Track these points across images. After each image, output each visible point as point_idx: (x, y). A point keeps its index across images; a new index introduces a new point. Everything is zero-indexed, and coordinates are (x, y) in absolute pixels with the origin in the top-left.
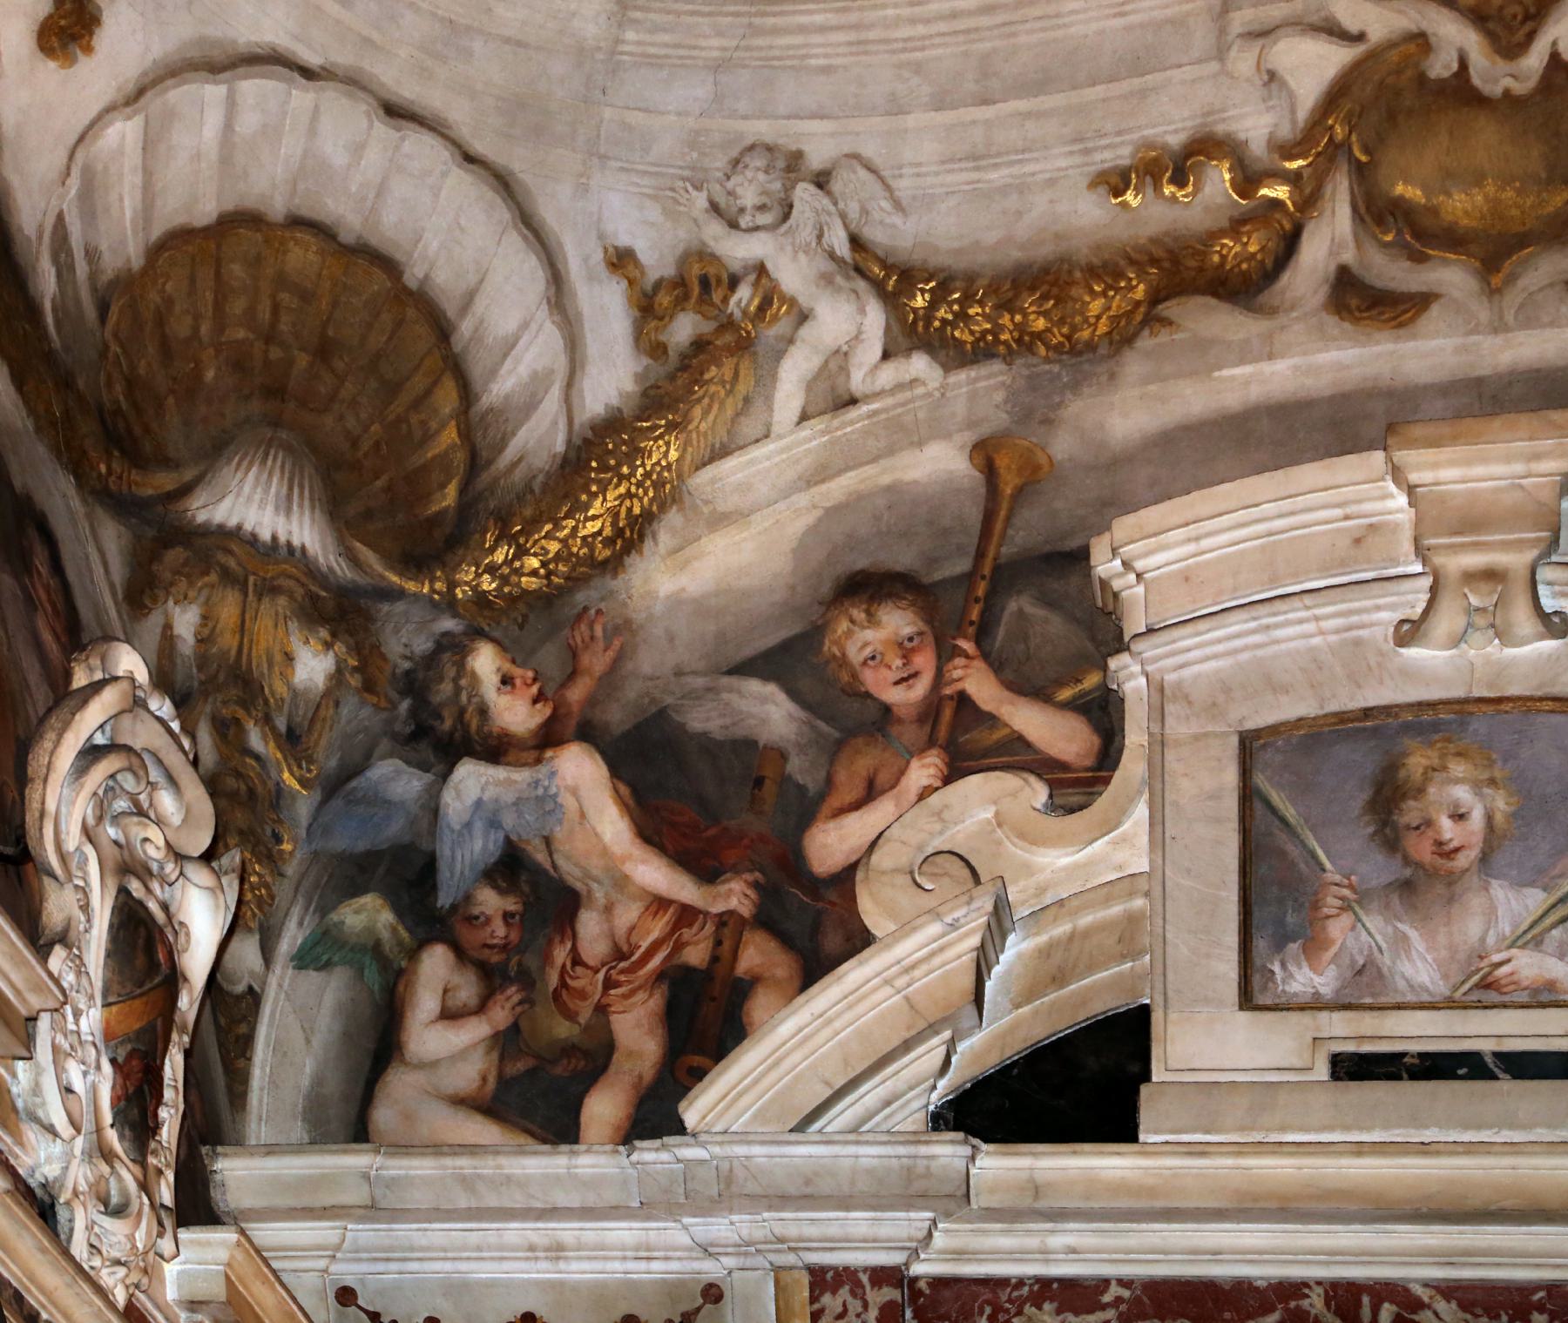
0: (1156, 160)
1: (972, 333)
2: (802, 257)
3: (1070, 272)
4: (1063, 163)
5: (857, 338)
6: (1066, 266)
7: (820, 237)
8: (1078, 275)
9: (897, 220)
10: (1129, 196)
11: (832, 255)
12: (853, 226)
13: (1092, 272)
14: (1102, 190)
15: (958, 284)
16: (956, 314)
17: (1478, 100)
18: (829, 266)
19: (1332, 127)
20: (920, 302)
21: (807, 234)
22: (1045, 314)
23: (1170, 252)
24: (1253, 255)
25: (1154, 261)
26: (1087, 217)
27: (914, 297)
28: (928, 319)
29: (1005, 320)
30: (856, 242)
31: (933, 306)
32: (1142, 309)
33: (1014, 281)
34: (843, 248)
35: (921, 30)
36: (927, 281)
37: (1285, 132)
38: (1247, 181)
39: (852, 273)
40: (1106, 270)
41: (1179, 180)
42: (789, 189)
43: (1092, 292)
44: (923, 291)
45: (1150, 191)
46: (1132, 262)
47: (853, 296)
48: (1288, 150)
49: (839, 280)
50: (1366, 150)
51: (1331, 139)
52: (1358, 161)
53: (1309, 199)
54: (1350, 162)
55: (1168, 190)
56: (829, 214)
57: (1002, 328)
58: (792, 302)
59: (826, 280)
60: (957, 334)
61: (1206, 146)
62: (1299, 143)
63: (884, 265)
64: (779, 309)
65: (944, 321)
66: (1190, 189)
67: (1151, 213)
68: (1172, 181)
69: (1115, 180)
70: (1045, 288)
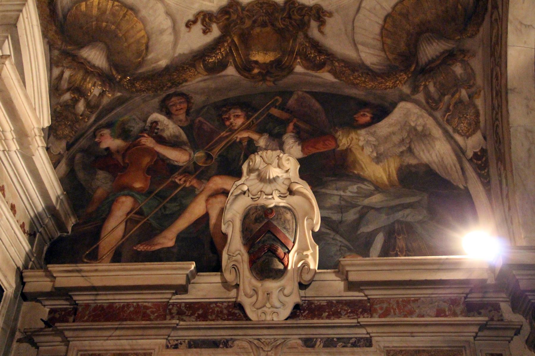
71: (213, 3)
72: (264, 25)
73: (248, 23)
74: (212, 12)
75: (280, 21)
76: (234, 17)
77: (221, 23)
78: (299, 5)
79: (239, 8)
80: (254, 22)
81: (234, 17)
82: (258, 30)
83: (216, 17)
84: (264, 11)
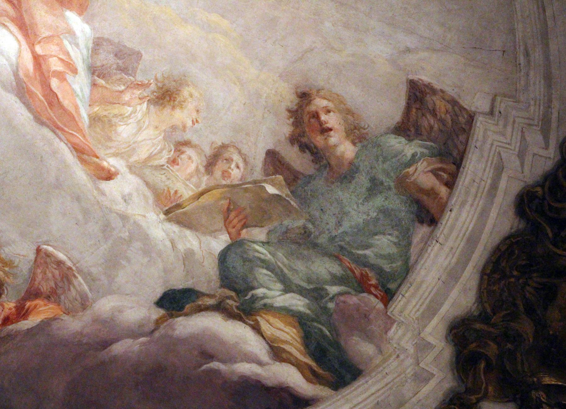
71: (433, 375)
72: (549, 294)
73: (526, 327)
74: (451, 390)
75: (559, 252)
76: (492, 349)
77: (490, 389)
78: (542, 186)
79: (478, 326)
80: (530, 310)
81: (492, 349)
82: (554, 315)
83: (468, 391)
84: (515, 273)
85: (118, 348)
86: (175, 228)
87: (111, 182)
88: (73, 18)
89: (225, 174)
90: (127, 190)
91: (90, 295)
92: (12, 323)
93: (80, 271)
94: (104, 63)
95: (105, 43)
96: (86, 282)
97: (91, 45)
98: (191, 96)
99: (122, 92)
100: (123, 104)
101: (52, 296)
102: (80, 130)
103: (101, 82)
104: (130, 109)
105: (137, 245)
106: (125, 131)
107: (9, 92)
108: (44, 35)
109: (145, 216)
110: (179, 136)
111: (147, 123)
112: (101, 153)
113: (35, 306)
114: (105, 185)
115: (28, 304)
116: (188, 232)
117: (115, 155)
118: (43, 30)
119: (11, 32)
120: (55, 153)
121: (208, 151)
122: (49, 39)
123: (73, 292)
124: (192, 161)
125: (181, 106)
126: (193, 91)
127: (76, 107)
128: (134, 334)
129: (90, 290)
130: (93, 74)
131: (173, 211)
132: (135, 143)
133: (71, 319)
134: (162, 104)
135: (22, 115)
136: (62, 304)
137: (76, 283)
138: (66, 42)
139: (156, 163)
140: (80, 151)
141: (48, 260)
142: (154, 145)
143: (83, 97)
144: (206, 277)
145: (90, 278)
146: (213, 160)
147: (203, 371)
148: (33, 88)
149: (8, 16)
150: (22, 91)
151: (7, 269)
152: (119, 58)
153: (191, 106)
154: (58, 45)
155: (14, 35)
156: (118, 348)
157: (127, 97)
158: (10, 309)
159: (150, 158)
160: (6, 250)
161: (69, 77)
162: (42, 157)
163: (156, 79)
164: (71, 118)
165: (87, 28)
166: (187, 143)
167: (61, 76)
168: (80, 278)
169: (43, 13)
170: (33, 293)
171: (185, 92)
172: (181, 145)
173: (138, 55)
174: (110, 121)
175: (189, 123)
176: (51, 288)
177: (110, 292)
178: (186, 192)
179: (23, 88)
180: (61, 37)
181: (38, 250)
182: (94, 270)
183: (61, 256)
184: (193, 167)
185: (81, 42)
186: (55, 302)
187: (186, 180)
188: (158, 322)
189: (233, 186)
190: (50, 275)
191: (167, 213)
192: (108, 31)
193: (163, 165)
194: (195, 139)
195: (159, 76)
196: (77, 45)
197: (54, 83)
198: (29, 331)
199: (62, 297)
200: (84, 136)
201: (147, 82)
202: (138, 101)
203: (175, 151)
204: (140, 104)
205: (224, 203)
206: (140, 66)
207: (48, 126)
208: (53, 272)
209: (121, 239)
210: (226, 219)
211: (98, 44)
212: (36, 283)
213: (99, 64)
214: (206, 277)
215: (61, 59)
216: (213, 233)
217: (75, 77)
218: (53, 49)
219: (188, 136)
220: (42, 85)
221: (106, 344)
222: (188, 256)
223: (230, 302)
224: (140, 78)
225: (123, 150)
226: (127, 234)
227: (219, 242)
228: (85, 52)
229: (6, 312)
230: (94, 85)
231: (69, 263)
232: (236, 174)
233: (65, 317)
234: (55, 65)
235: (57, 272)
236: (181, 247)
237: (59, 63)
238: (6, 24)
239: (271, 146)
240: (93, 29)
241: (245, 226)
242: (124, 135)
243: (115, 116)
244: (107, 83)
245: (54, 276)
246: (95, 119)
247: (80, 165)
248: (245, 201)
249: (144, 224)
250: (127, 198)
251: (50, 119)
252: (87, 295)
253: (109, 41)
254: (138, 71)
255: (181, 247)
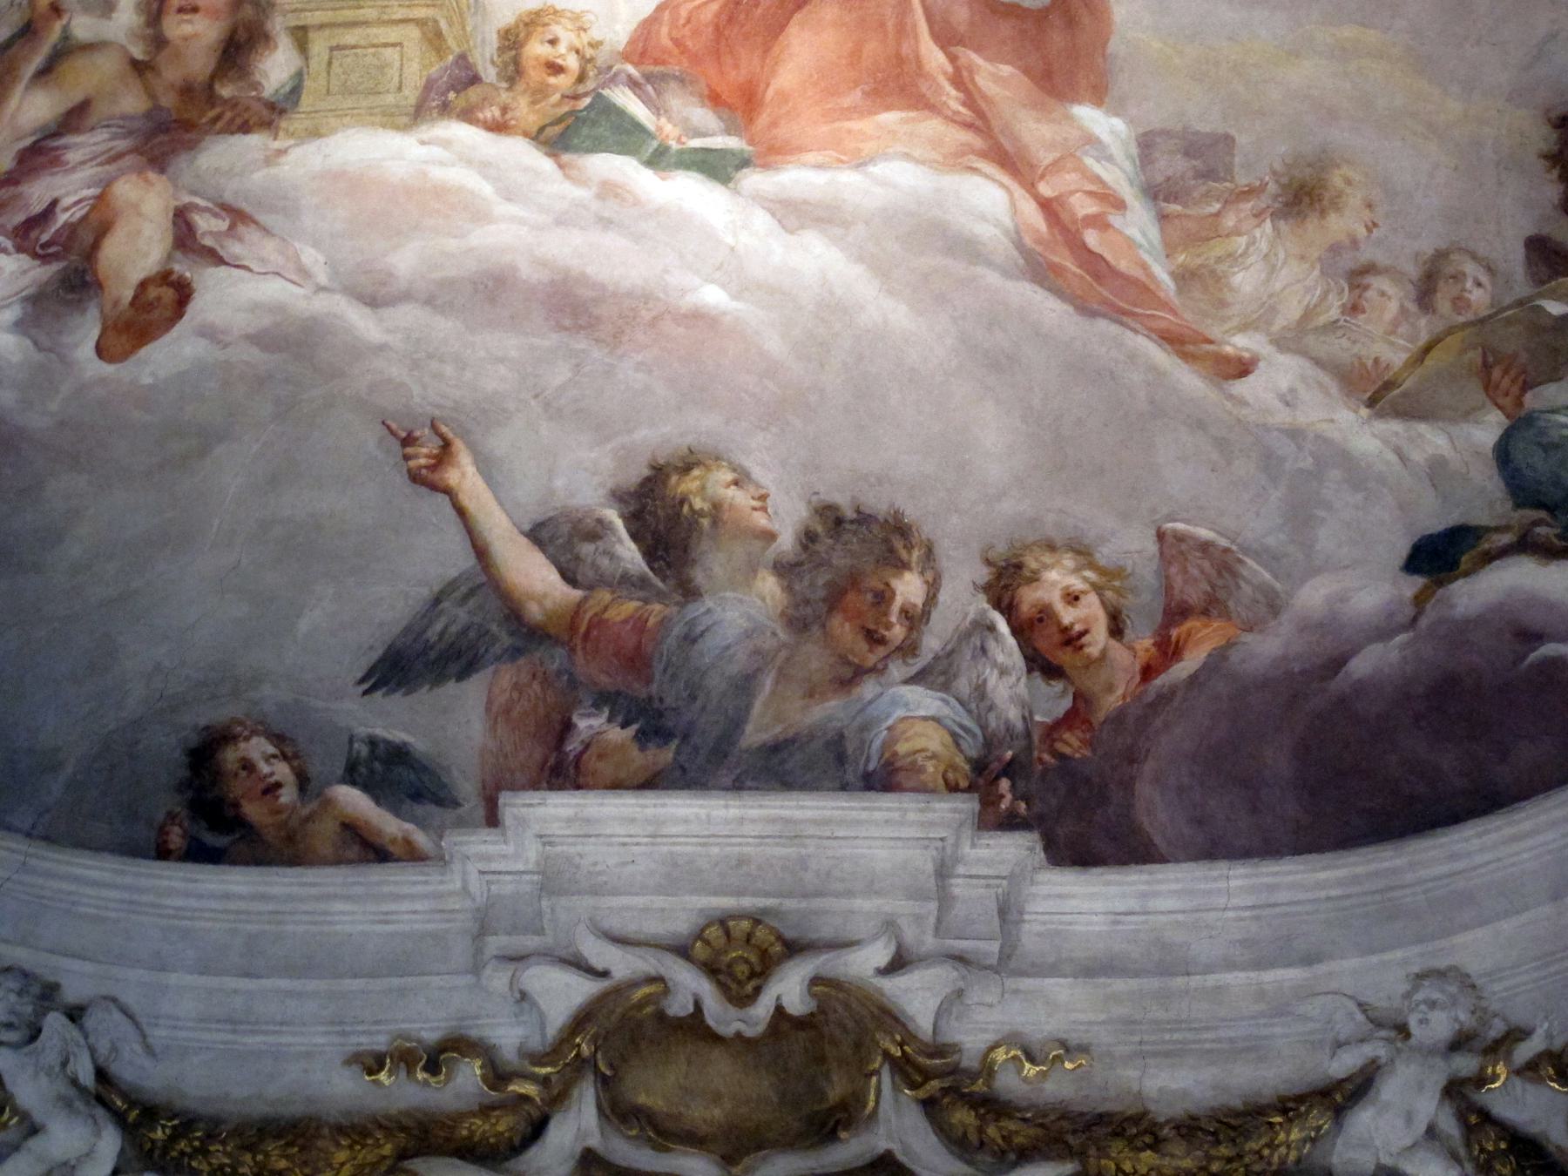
0: (410, 1051)
1: (210, 1164)
2: (44, 1080)
3: (318, 1128)
4: (321, 1040)
5: (89, 1154)
6: (314, 1124)
7: (64, 1064)
8: (326, 1131)
9: (147, 1063)
10: (383, 1076)
11: (74, 1082)
12: (101, 1060)
13: (340, 1130)
14: (356, 1068)
15: (201, 1125)
16: (196, 1150)
17: (715, 1038)
18: (71, 1092)
19: (579, 1045)
20: (159, 1134)
21: (52, 1058)
22: (287, 1157)
23: (420, 1123)
24: (502, 1133)
25: (403, 1129)
26: (342, 1089)
27: (154, 1130)
28: (166, 1149)
29: (248, 1157)
30: (101, 1075)
31: (173, 1139)
32: (388, 1162)
33: (259, 1130)
34: (87, 1077)
35: (193, 903)
36: (170, 1119)
37: (535, 1044)
38: (498, 1076)
39: (93, 1102)
40: (356, 1130)
41: (433, 1067)
42: (41, 1013)
43: (338, 1145)
44: (164, 1127)
45: (403, 1074)
46: (380, 1126)
47: (90, 1121)
48: (538, 1060)
49: (79, 1104)
50: (611, 1066)
51: (578, 1055)
52: (604, 1075)
53: (557, 1098)
54: (596, 1074)
55: (421, 1075)
56: (78, 1046)
57: (242, 1164)
58: (25, 1116)
59: (68, 1104)
60: (194, 1164)
61: (457, 1046)
62: (548, 1054)
63: (125, 1096)
64: (10, 1118)
65: (182, 1153)
66: (442, 1077)
67: (401, 1092)
68: (425, 1069)
69: (370, 1061)
70: (290, 1137)
85: (1361, 666)
86: (1395, 426)
87: (1251, 378)
88: (1088, 115)
89: (1459, 303)
90: (1284, 385)
91: (1278, 586)
92: (1159, 673)
93: (1246, 550)
94: (1170, 173)
95: (1158, 140)
96: (1266, 567)
97: (1134, 151)
98: (1349, 182)
99: (1218, 214)
100: (1227, 236)
101: (1212, 607)
102: (1165, 305)
103: (1175, 208)
104: (1243, 240)
105: (1335, 474)
106: (1245, 281)
107: (1018, 279)
108: (1046, 162)
109: (1332, 421)
110: (1347, 261)
111: (1282, 255)
112: (1215, 332)
113: (1189, 634)
114: (1241, 387)
115: (1174, 633)
116: (1422, 427)
117: (1244, 328)
118: (1042, 154)
119: (987, 176)
120: (1133, 357)
121: (1413, 271)
122: (1056, 166)
123: (1247, 589)
124: (1389, 298)
125: (1336, 205)
126: (1350, 174)
127: (1145, 267)
128: (1383, 634)
129: (1276, 577)
130: (1155, 198)
131: (1380, 395)
132: (1271, 296)
133: (1259, 637)
134: (1298, 213)
135: (1050, 309)
136: (1234, 615)
137: (1245, 573)
138: (1089, 161)
139: (1322, 320)
140: (1177, 341)
141: (1184, 547)
142: (1308, 290)
143: (1150, 243)
144: (1483, 499)
145: (1270, 558)
146: (1428, 285)
147: (1531, 666)
148: (1056, 259)
149: (973, 152)
150: (1040, 272)
151: (1117, 583)
152: (1195, 158)
153: (1354, 199)
154: (1074, 170)
155: (994, 180)
156: (1361, 666)
157: (1230, 221)
158: (1147, 650)
159: (1308, 315)
160: (1105, 550)
161: (1115, 219)
162: (1112, 373)
163: (1274, 173)
164: (1143, 289)
165: (1118, 124)
166: (1369, 269)
167: (1099, 222)
168: (1249, 562)
169: (1034, 126)
170: (1177, 612)
171: (1336, 180)
172: (1359, 276)
173: (1228, 140)
174: (1213, 272)
175: (1361, 232)
176: (1206, 593)
177: (1314, 571)
178: (1395, 356)
179: (1040, 264)
180: (1078, 154)
181: (1161, 536)
182: (1271, 541)
183: (1204, 533)
184: (1393, 308)
185: (1116, 150)
186: (1220, 616)
187: (1387, 334)
188: (1420, 600)
189: (1482, 321)
190: (1195, 572)
191: (1371, 403)
192: (1157, 118)
193: (1337, 321)
194: (1381, 257)
195: (1278, 166)
196: (1110, 159)
197: (1092, 238)
198: (1193, 679)
199: (1231, 604)
200: (1174, 313)
201: (1258, 183)
202: (1254, 221)
203: (1351, 289)
204: (1258, 226)
205: (1475, 356)
206: (1237, 159)
207: (1104, 316)
208: (1199, 566)
209: (1305, 478)
210: (1489, 387)
211: (1147, 145)
212: (1176, 592)
213: (1160, 179)
214: (1483, 499)
215: (1090, 193)
216: (1468, 415)
217: (1124, 215)
218: (1070, 179)
219: (1367, 254)
220: (1071, 249)
221: (1337, 663)
222: (1437, 470)
223: (1541, 530)
224: (1243, 180)
225: (1255, 316)
226: (1310, 460)
227: (1487, 430)
228: (1127, 165)
229: (1143, 657)
230: (1163, 218)
231: (1223, 542)
232: (1479, 298)
233: (1248, 638)
234: (1083, 206)
235: (1206, 564)
236: (1417, 456)
237: (1088, 201)
238: (975, 165)
239: (1530, 230)
240: (1131, 122)
241: (1526, 387)
242: (1248, 289)
243: (1219, 260)
244: (1185, 206)
245: (1202, 572)
246: (1184, 277)
247: (1184, 365)
248: (1512, 342)
249: (1336, 435)
250: (1289, 398)
251: (1105, 302)
252: (1273, 589)
253: (1165, 133)
254: (1236, 169)
255: (1417, 456)
